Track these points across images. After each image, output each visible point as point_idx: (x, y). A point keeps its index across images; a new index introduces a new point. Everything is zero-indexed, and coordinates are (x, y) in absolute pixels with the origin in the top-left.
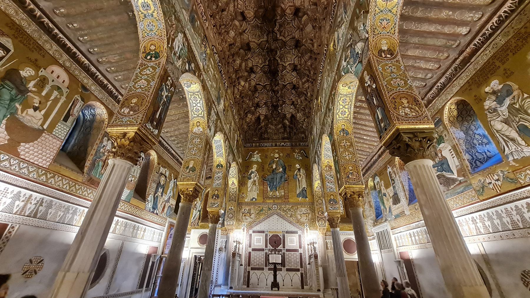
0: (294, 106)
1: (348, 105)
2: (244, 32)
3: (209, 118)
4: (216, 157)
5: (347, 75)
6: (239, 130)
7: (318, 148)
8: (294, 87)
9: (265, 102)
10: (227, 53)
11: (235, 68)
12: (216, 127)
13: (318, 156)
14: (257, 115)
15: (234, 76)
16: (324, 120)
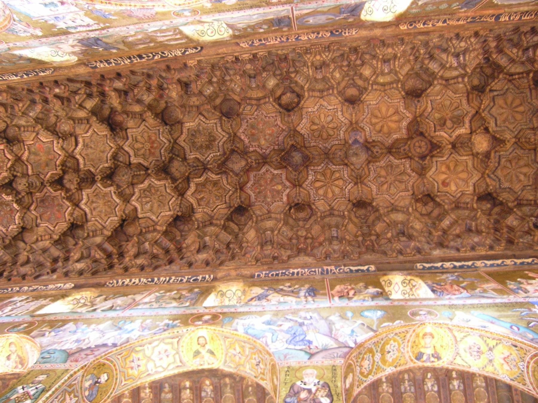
0: (21, 233)
1: (156, 367)
2: (201, 114)
9: (24, 158)
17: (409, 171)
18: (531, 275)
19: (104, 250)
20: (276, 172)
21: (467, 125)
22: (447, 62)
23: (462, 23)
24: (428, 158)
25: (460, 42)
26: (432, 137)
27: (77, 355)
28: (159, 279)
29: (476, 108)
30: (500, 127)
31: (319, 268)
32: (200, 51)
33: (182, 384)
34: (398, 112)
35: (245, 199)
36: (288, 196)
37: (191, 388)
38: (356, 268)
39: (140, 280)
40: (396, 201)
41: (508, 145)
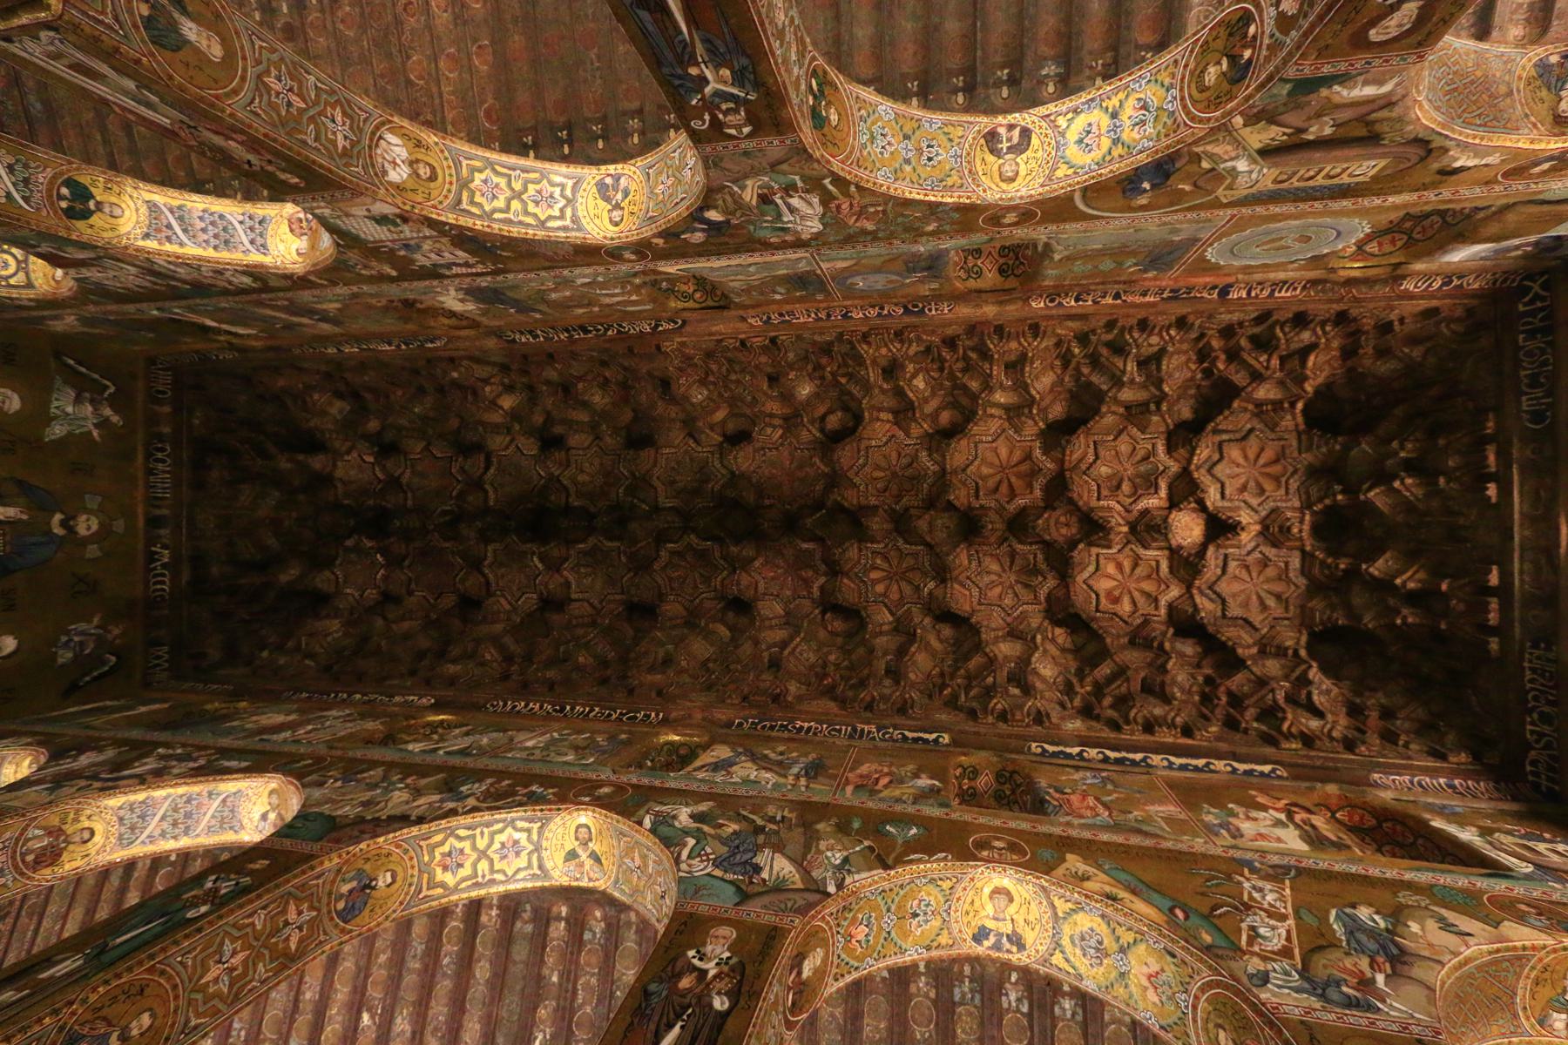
1: (492, 871)
2: (691, 435)
3: (443, 233)
4: (148, 196)
5: (649, 841)
6: (270, 349)
7: (180, 758)
8: (469, 605)
9: (404, 480)
10: (644, 368)
11: (580, 386)
12: (373, 251)
13: (117, 766)
14: (337, 444)
15: (551, 374)
16: (373, 764)
17: (1044, 567)
18: (1261, 799)
19: (502, 648)
20: (805, 546)
21: (1163, 493)
22: (1124, 372)
23: (1152, 299)
24: (1081, 546)
25: (1149, 336)
26: (1092, 509)
27: (348, 830)
28: (572, 709)
29: (1184, 462)
30: (1231, 500)
31: (847, 725)
32: (680, 327)
33: (555, 909)
34: (1031, 459)
35: (748, 587)
36: (822, 588)
37: (567, 920)
38: (916, 735)
39: (541, 707)
40: (1015, 618)
41: (1244, 537)
